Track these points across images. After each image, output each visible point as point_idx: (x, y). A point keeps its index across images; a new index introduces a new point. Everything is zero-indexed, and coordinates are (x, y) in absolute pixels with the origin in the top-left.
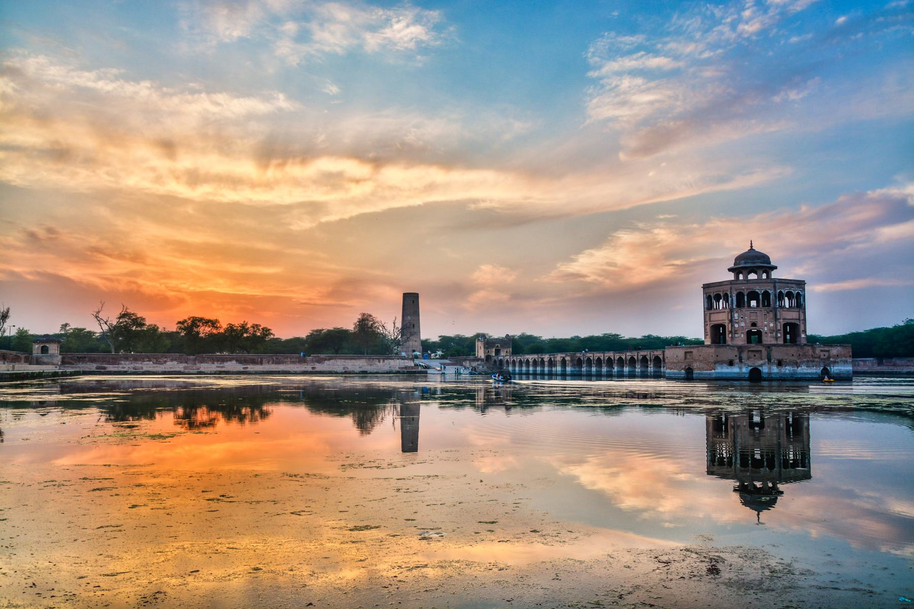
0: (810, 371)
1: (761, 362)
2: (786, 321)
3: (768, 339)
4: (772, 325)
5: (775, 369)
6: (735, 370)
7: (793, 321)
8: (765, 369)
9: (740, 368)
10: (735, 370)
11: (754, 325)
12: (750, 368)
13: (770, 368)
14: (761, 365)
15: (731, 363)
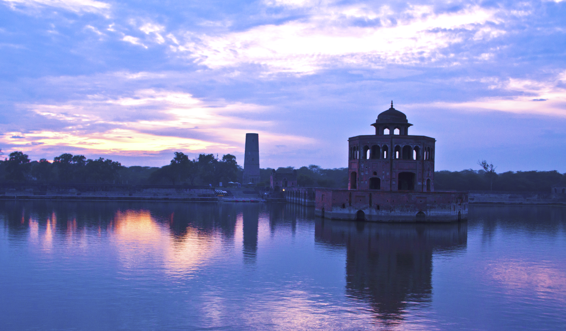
0: (403, 214)
1: (364, 206)
2: (401, 171)
3: (384, 185)
4: (388, 174)
5: (374, 212)
6: (346, 211)
7: (409, 171)
8: (367, 212)
9: (350, 210)
10: (346, 211)
11: (375, 173)
12: (357, 210)
13: (371, 211)
14: (364, 209)
15: (344, 206)
